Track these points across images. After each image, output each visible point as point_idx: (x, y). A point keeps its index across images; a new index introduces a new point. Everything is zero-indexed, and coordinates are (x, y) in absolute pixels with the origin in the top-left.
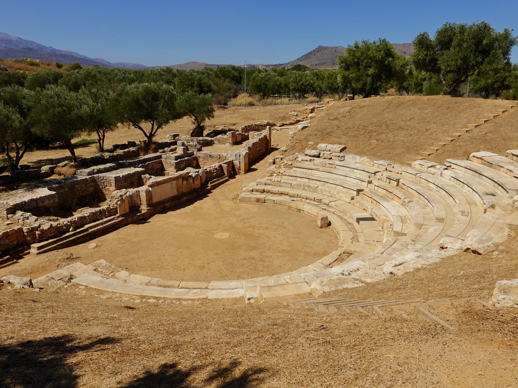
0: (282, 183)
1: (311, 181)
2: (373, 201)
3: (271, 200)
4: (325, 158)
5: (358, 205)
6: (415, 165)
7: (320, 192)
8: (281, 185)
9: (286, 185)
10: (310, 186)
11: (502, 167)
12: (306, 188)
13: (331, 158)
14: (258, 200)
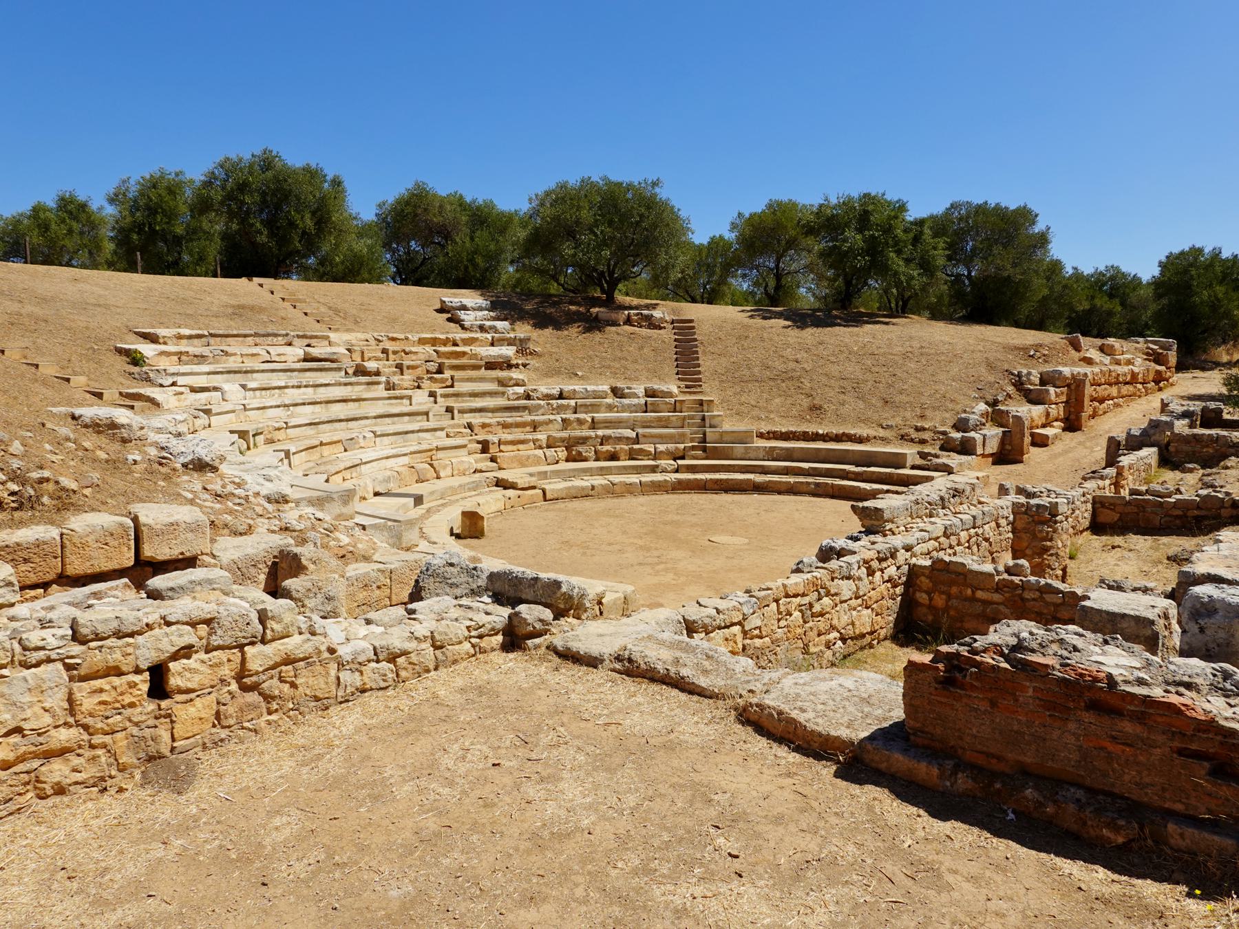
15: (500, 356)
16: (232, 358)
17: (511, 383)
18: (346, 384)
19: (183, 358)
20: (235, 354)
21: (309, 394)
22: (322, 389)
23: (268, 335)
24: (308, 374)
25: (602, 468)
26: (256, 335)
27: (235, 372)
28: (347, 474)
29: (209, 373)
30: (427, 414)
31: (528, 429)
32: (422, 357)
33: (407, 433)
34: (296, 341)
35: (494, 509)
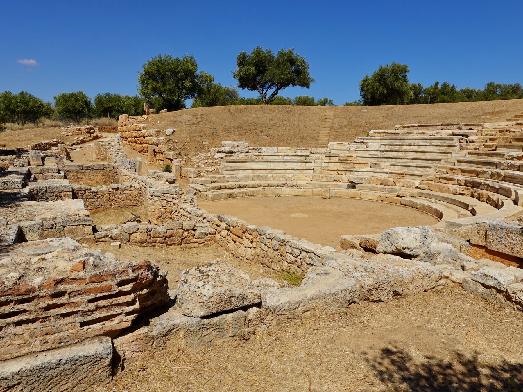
0: (228, 178)
1: (255, 172)
2: (339, 172)
4: (241, 153)
5: (324, 179)
7: (272, 180)
8: (228, 180)
9: (233, 180)
11: (411, 133)
12: (255, 179)
13: (248, 152)
16: (412, 134)
18: (436, 146)
19: (386, 134)
21: (416, 148)
24: (435, 141)
27: (395, 139)
28: (343, 173)
29: (381, 139)
30: (440, 160)
31: (474, 175)
32: (517, 134)
33: (409, 166)
35: (370, 198)
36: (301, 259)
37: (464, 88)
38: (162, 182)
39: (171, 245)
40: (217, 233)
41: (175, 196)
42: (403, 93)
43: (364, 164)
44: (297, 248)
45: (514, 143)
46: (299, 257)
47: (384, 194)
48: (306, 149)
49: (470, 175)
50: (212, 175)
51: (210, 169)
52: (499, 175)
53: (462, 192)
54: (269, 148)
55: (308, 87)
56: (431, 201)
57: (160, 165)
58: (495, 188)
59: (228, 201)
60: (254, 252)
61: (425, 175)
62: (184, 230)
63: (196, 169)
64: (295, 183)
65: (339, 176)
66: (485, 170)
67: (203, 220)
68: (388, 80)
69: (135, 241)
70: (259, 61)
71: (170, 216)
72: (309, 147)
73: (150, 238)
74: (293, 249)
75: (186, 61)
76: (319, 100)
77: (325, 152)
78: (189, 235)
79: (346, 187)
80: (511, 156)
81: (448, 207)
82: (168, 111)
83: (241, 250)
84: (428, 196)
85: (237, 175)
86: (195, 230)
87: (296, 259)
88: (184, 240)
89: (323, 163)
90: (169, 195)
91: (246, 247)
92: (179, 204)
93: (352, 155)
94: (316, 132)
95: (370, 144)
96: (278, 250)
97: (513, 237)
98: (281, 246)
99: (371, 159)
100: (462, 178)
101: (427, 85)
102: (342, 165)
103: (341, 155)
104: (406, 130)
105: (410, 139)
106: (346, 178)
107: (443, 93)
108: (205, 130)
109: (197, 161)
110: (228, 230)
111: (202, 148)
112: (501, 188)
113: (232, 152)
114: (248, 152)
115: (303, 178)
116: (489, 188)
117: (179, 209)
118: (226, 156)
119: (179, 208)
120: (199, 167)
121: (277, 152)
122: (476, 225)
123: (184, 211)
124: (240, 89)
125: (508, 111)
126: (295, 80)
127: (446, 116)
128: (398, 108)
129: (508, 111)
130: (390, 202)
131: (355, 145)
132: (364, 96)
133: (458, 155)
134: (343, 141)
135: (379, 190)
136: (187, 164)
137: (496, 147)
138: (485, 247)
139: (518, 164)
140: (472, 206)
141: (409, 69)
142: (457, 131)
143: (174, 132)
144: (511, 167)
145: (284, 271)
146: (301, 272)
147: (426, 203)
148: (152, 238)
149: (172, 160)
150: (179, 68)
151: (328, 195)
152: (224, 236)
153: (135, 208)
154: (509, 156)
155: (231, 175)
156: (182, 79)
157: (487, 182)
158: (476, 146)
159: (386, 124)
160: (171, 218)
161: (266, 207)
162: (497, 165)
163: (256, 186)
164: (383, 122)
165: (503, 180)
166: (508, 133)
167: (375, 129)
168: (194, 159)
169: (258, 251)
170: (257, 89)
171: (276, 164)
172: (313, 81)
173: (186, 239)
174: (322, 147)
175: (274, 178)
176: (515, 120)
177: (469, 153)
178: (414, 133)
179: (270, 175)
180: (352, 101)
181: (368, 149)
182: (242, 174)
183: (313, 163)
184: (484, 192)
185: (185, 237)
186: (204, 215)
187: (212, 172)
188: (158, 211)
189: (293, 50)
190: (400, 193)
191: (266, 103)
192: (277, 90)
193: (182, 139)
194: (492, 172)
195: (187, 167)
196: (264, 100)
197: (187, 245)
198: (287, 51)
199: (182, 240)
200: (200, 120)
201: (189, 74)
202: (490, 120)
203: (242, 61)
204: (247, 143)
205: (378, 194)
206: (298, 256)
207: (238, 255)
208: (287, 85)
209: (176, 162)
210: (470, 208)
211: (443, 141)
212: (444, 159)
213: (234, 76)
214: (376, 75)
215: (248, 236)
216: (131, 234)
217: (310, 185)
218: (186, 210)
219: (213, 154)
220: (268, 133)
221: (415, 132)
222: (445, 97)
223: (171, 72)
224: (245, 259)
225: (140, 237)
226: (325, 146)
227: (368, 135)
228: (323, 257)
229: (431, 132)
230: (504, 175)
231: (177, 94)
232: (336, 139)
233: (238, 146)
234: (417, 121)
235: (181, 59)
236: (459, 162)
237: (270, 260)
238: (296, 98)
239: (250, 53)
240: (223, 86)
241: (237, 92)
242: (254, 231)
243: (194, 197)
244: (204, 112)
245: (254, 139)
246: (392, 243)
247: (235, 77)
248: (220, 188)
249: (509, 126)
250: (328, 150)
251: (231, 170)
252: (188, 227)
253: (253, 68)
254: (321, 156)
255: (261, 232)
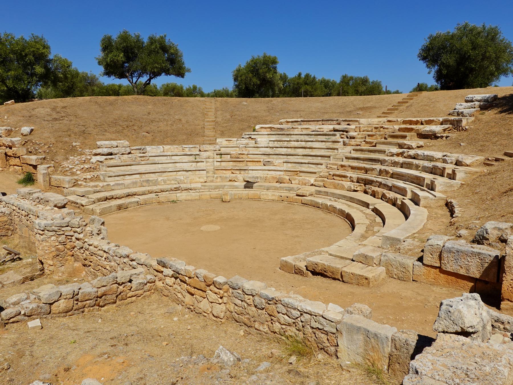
0: (113, 185)
1: (143, 176)
2: (233, 171)
3: (134, 202)
4: (123, 154)
5: (219, 180)
6: (221, 142)
7: (163, 183)
8: (113, 188)
9: (119, 187)
10: (148, 180)
11: (295, 128)
12: (144, 184)
13: (130, 153)
14: (120, 208)
15: (430, 131)
17: (406, 147)
18: (322, 141)
19: (273, 129)
20: (297, 128)
21: (303, 144)
22: (310, 143)
23: (328, 120)
24: (319, 137)
25: (351, 198)
26: (322, 120)
27: (282, 135)
28: (238, 172)
29: (268, 135)
30: (329, 157)
31: (363, 171)
32: (391, 130)
33: (302, 163)
34: (342, 123)
35: (270, 198)
36: (302, 322)
37: (321, 79)
38: (48, 208)
39: (103, 306)
40: (157, 280)
41: (79, 230)
42: (274, 84)
43: (257, 161)
44: (295, 309)
45: (390, 140)
46: (299, 319)
47: (285, 194)
48: (195, 147)
49: (360, 171)
50: (92, 184)
51: (88, 176)
52: (387, 172)
53: (356, 189)
54: (153, 147)
55: (183, 77)
56: (330, 200)
57: (16, 172)
58: (388, 186)
59: (119, 215)
60: (224, 308)
61: (318, 172)
62: (119, 284)
63: (70, 178)
64: (189, 186)
65: (234, 175)
66: (374, 167)
67: (131, 263)
68: (261, 71)
69: (57, 312)
70: (127, 47)
71: (71, 253)
72: (196, 144)
73: (77, 304)
74: (289, 309)
75: (35, 42)
76: (188, 87)
77: (215, 149)
78: (125, 288)
79: (243, 187)
80: (391, 153)
81: (349, 206)
82: (16, 102)
83: (204, 305)
84: (326, 194)
85: (122, 182)
86: (130, 281)
87: (294, 321)
88: (120, 296)
89: (215, 163)
90: (69, 228)
91: (211, 303)
92: (86, 240)
93: (244, 152)
94: (200, 127)
95: (259, 140)
96: (263, 309)
97: (469, 260)
98: (269, 304)
99: (263, 156)
100: (355, 175)
101: (291, 75)
102: (234, 164)
103: (232, 152)
104: (290, 125)
105: (296, 135)
106: (241, 177)
107: (306, 84)
108: (72, 127)
109: (70, 167)
110: (176, 278)
111: (73, 150)
112: (394, 186)
113: (111, 154)
114: (130, 153)
115: (196, 181)
116: (382, 186)
117: (86, 245)
118: (106, 159)
119: (86, 244)
120: (73, 174)
121: (163, 152)
122: (429, 247)
123: (96, 249)
124: (106, 77)
125: (375, 107)
126: (168, 70)
127: (323, 111)
128: (277, 102)
129: (375, 107)
130: (290, 201)
131: (245, 141)
132: (237, 86)
133: (343, 151)
134: (230, 137)
135: (276, 189)
136: (56, 171)
137: (376, 144)
138: (440, 268)
139: (401, 162)
140: (373, 205)
141: (279, 60)
142: (337, 127)
143: (32, 130)
144: (395, 164)
145: (275, 333)
146: (302, 335)
147: (329, 203)
148: (79, 303)
149: (35, 167)
150: (27, 50)
151: (228, 198)
152: (171, 284)
153: (4, 238)
154: (390, 152)
155: (119, 182)
156: (32, 64)
157: (379, 180)
158: (358, 141)
159: (269, 118)
160: (73, 256)
161: (168, 219)
162: (382, 162)
163: (147, 193)
164: (266, 116)
165: (392, 177)
166: (382, 129)
167: (260, 124)
168: (65, 164)
169: (232, 307)
170: (127, 77)
171: (165, 165)
172: (189, 71)
173: (122, 294)
174: (210, 144)
175: (165, 181)
176: (384, 117)
177: (354, 150)
178: (299, 129)
179: (160, 179)
180: (219, 88)
181: (258, 146)
182: (128, 180)
183: (205, 163)
184: (376, 189)
185: (120, 294)
186: (132, 256)
187: (91, 180)
188: (54, 249)
189: (165, 36)
190: (300, 192)
191: (139, 94)
192: (149, 80)
193: (44, 139)
194: (380, 170)
195: (58, 174)
196: (136, 90)
197: (123, 301)
198: (158, 37)
199: (117, 297)
200: (63, 115)
201: (41, 57)
202: (363, 117)
203: (107, 46)
204: (127, 143)
205: (277, 193)
206: (297, 318)
207: (200, 311)
208: (159, 74)
209: (42, 169)
210: (371, 207)
211: (327, 137)
212: (333, 155)
213: (99, 62)
214: (248, 66)
215: (217, 291)
216: (51, 304)
217: (206, 187)
218: (99, 248)
219: (89, 157)
220: (148, 129)
221: (300, 127)
222: (308, 88)
223: (15, 54)
224: (211, 316)
225: (65, 305)
226: (213, 143)
227: (254, 130)
228: (339, 322)
229: (314, 127)
230: (392, 172)
231: (26, 82)
232: (222, 134)
233: (117, 147)
234: (299, 115)
235: (28, 39)
236: (346, 158)
237: (252, 319)
238: (163, 85)
239: (115, 37)
240: (80, 71)
241: (97, 79)
242: (225, 285)
243: (102, 227)
244: (65, 105)
245: (134, 136)
246: (457, 323)
247: (100, 63)
248: (106, 199)
249: (381, 123)
250: (218, 147)
251: (115, 176)
252: (123, 281)
253: (122, 55)
254: (212, 155)
255: (235, 285)
